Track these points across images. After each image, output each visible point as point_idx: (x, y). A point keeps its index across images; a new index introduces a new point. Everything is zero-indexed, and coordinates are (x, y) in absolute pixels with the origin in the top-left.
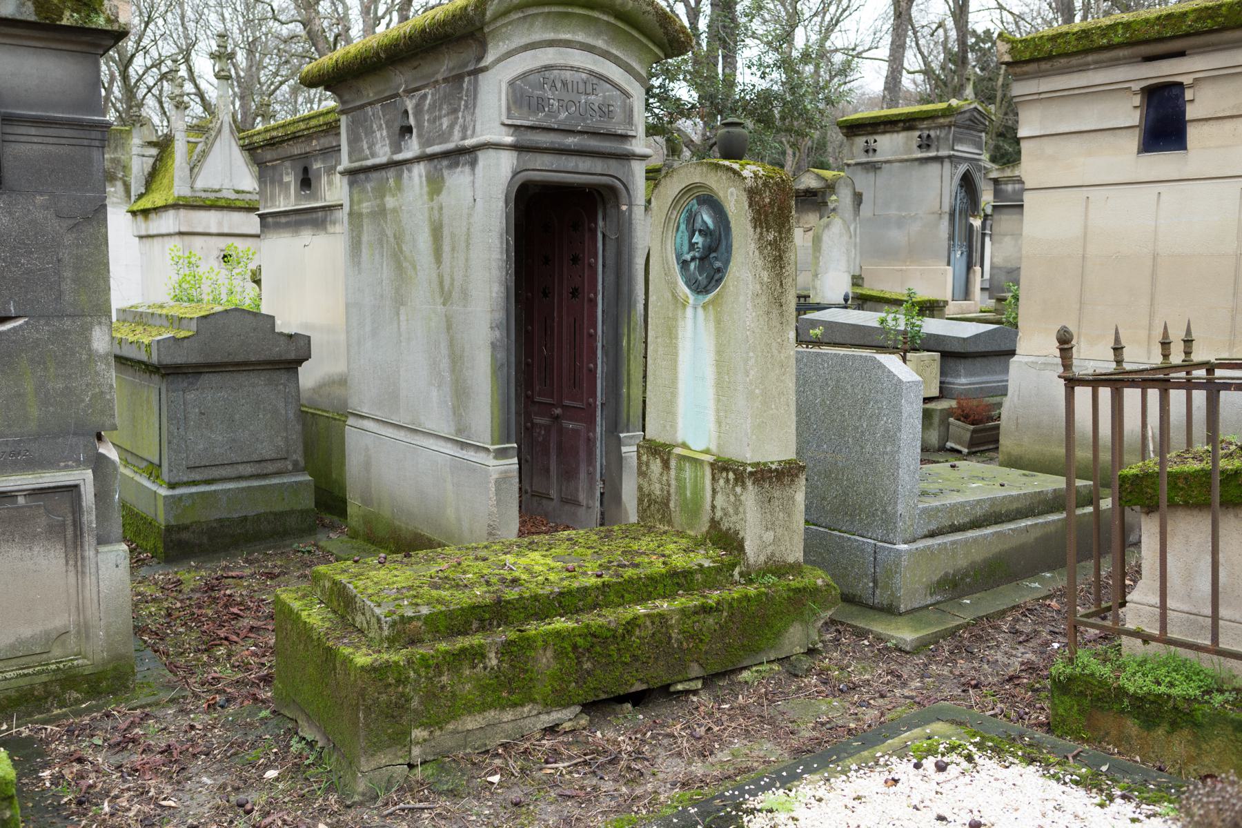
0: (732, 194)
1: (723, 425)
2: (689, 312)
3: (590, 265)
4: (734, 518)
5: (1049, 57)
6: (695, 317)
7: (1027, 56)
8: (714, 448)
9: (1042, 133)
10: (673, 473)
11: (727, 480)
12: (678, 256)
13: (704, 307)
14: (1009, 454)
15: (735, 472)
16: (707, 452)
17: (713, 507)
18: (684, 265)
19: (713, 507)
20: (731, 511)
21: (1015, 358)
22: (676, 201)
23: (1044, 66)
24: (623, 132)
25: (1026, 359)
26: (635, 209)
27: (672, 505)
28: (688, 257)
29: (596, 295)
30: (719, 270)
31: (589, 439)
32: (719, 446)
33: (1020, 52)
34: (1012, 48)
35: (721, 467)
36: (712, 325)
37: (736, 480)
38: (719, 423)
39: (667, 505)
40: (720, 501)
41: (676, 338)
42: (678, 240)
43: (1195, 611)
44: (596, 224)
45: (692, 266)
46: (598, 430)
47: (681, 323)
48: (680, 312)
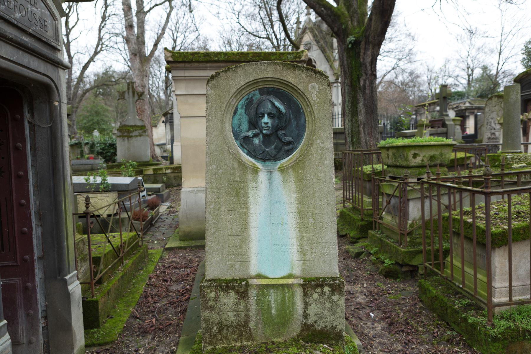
0: (313, 87)
1: (309, 256)
2: (263, 176)
3: (16, 148)
4: (332, 318)
5: (191, 62)
6: (270, 179)
7: (181, 60)
8: (297, 271)
9: (187, 93)
10: (252, 300)
11: (323, 293)
12: (236, 135)
13: (282, 170)
14: (184, 232)
15: (330, 286)
16: (290, 276)
17: (306, 316)
18: (245, 143)
19: (306, 316)
20: (327, 314)
21: (183, 190)
22: (239, 91)
23: (187, 65)
24: (55, 45)
25: (188, 190)
26: (62, 105)
27: (252, 325)
28: (250, 134)
29: (26, 172)
30: (289, 143)
31: (26, 288)
32: (303, 270)
33: (177, 57)
34: (173, 55)
35: (311, 284)
36: (292, 185)
37: (333, 292)
38: (303, 253)
39: (246, 324)
40: (313, 310)
41: (246, 195)
42: (236, 121)
43: (525, 284)
44: (22, 115)
45: (256, 141)
46: (37, 279)
47: (251, 185)
48: (250, 176)
